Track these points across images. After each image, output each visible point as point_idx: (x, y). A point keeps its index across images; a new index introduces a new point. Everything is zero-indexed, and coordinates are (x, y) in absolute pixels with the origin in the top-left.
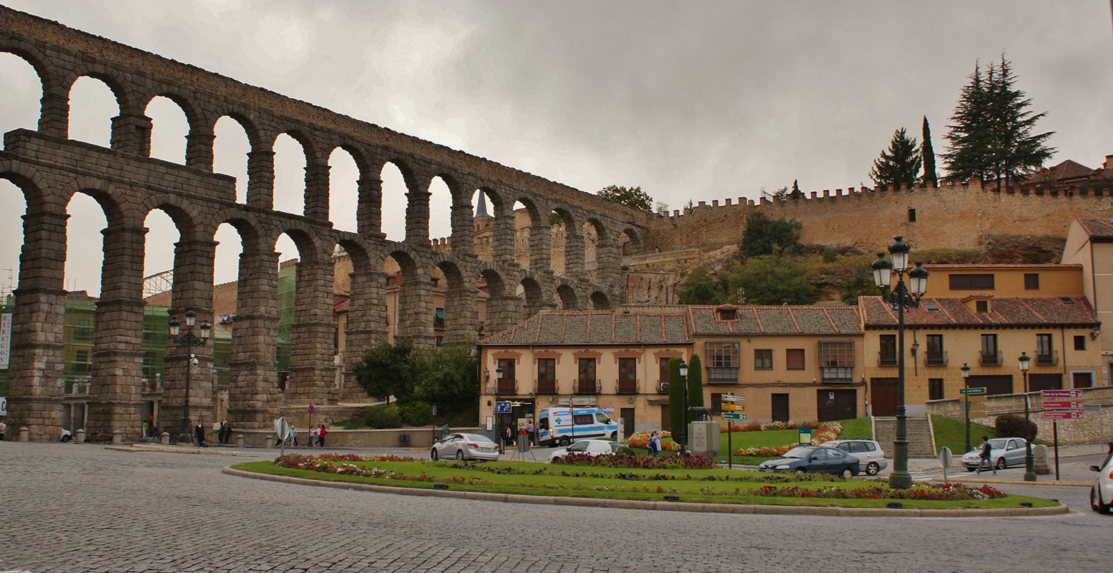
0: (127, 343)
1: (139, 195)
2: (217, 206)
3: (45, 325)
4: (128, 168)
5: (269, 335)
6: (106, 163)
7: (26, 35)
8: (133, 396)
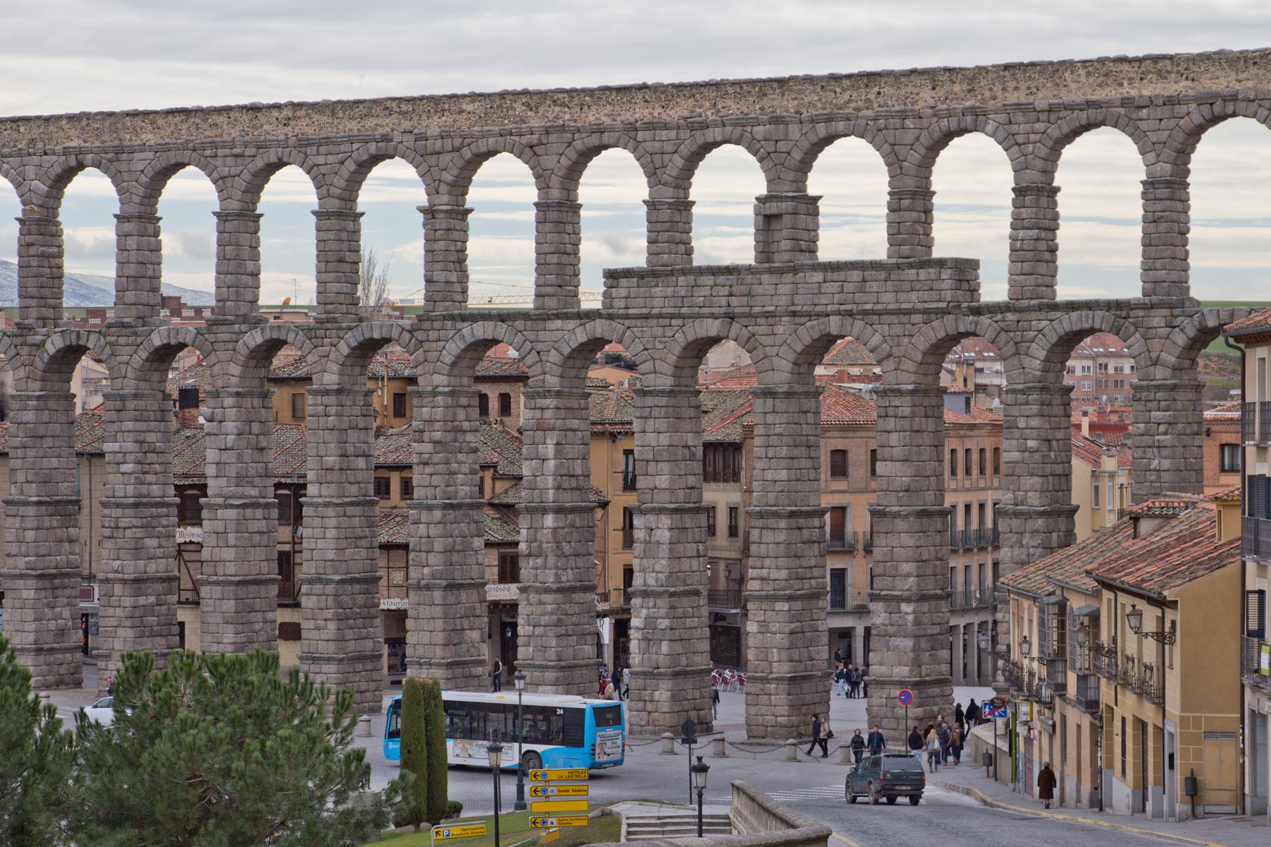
0: (762, 579)
1: (779, 329)
2: (917, 318)
3: (645, 561)
4: (760, 289)
5: (1022, 546)
6: (726, 291)
7: (607, 121)
8: (775, 664)
